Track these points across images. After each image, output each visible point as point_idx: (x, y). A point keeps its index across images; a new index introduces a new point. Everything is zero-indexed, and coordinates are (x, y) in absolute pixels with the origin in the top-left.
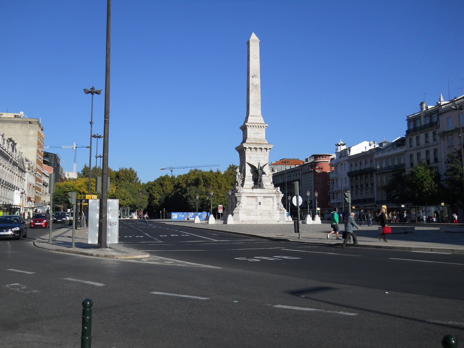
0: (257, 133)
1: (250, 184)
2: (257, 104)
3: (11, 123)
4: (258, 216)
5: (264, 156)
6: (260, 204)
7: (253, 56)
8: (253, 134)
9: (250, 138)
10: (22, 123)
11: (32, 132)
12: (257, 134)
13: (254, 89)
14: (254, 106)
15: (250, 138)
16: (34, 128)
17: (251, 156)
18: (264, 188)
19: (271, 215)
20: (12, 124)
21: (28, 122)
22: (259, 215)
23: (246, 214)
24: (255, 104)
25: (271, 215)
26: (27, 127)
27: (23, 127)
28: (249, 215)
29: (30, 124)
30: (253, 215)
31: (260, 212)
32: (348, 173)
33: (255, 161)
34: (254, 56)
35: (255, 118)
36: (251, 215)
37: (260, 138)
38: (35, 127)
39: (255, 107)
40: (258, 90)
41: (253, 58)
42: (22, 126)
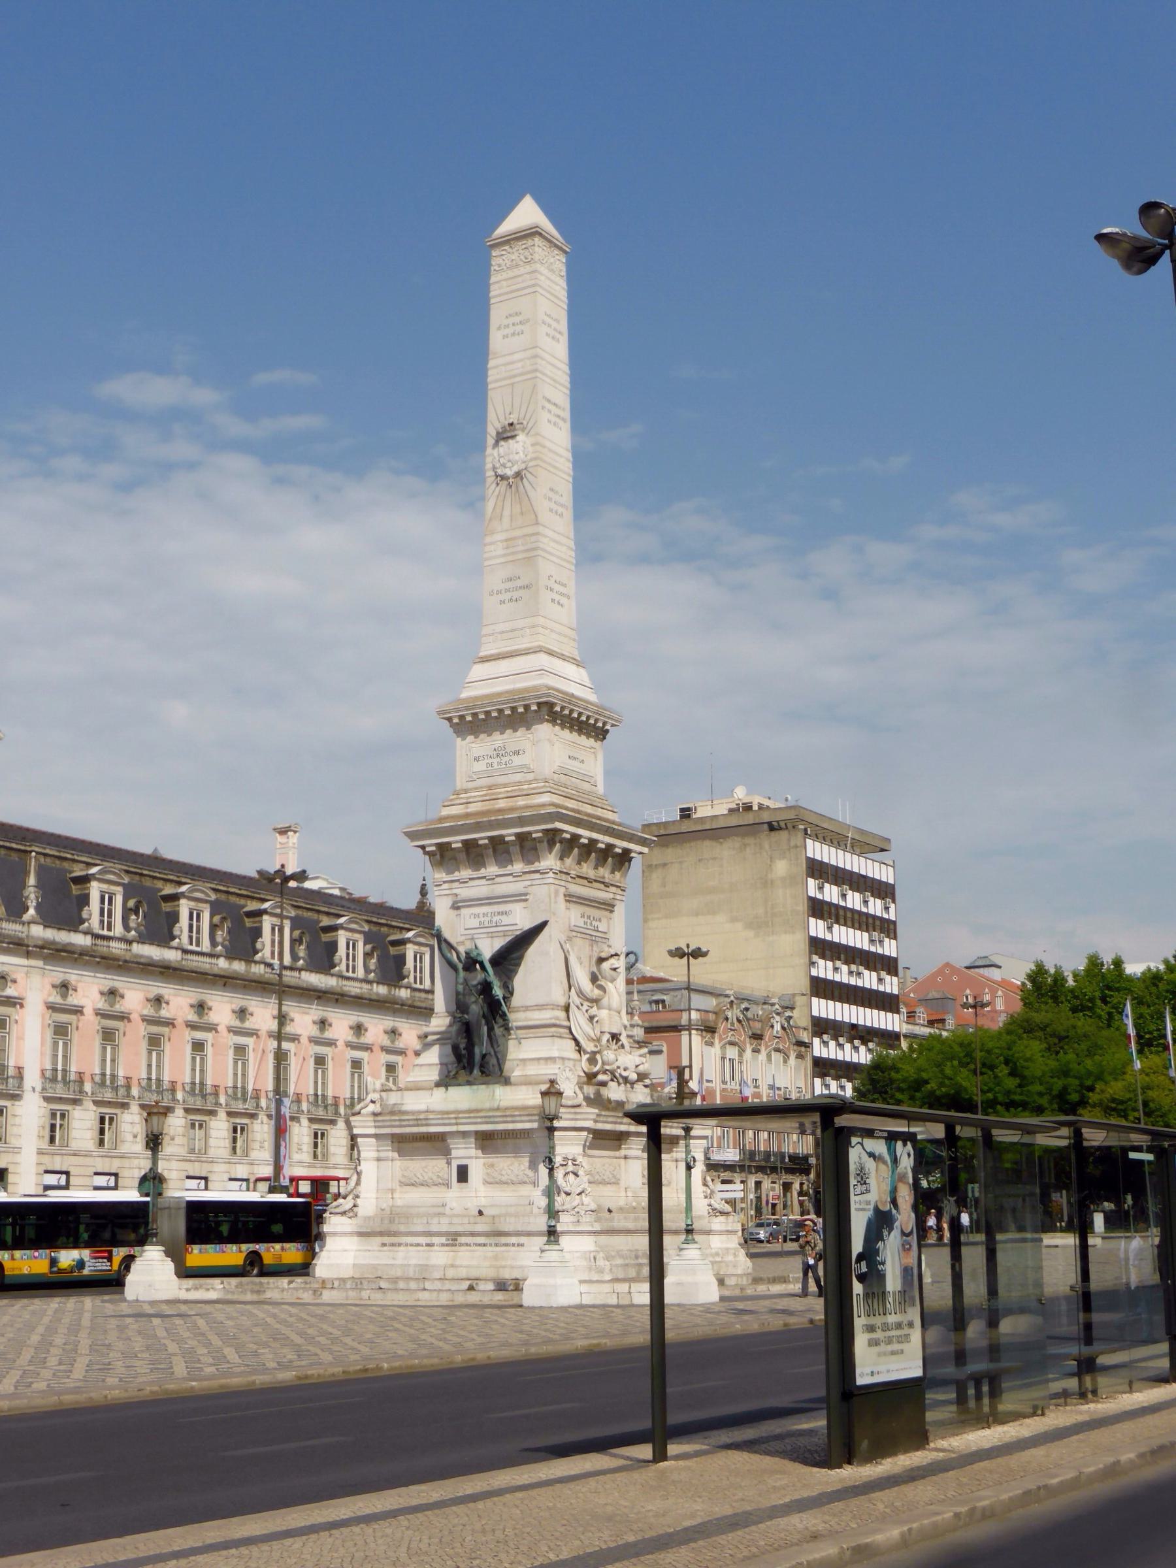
0: (500, 753)
2: (519, 583)
3: (704, 838)
4: (435, 1248)
5: (529, 883)
6: (463, 1174)
7: (506, 322)
8: (481, 766)
9: (466, 791)
10: (744, 835)
11: (781, 867)
12: (504, 760)
13: (507, 513)
14: (506, 596)
15: (471, 785)
16: (789, 850)
17: (464, 892)
18: (507, 1082)
19: (506, 1245)
20: (707, 843)
21: (766, 826)
22: (443, 1245)
23: (379, 1240)
24: (509, 585)
25: (506, 1245)
26: (761, 847)
27: (749, 851)
28: (393, 1245)
29: (773, 833)
30: (411, 1245)
31: (444, 1228)
33: (477, 920)
34: (511, 320)
35: (504, 666)
36: (400, 1245)
37: (518, 777)
38: (792, 843)
41: (507, 331)
42: (745, 845)
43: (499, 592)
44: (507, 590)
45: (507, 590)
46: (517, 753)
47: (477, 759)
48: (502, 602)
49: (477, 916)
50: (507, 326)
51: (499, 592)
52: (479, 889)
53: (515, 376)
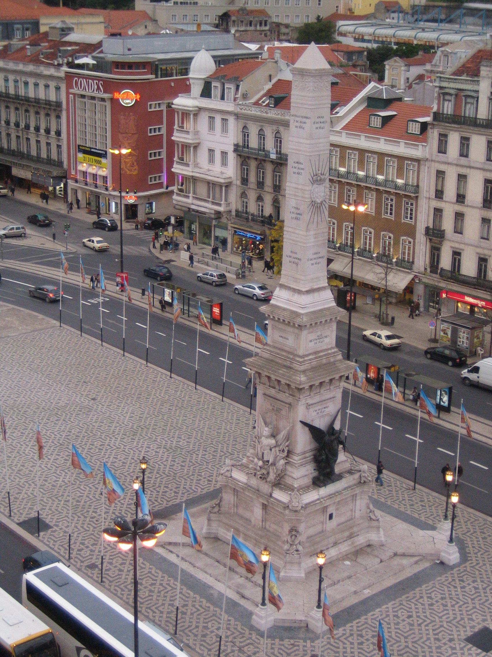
0: (320, 338)
1: (307, 473)
2: (320, 255)
13: (315, 220)
17: (310, 401)
24: (315, 256)
32: (235, 145)
39: (316, 263)
40: (323, 215)
43: (311, 259)
44: (315, 259)
45: (315, 259)
46: (326, 337)
47: (311, 341)
48: (312, 264)
49: (316, 411)
50: (317, 123)
51: (311, 259)
52: (317, 399)
53: (321, 151)
